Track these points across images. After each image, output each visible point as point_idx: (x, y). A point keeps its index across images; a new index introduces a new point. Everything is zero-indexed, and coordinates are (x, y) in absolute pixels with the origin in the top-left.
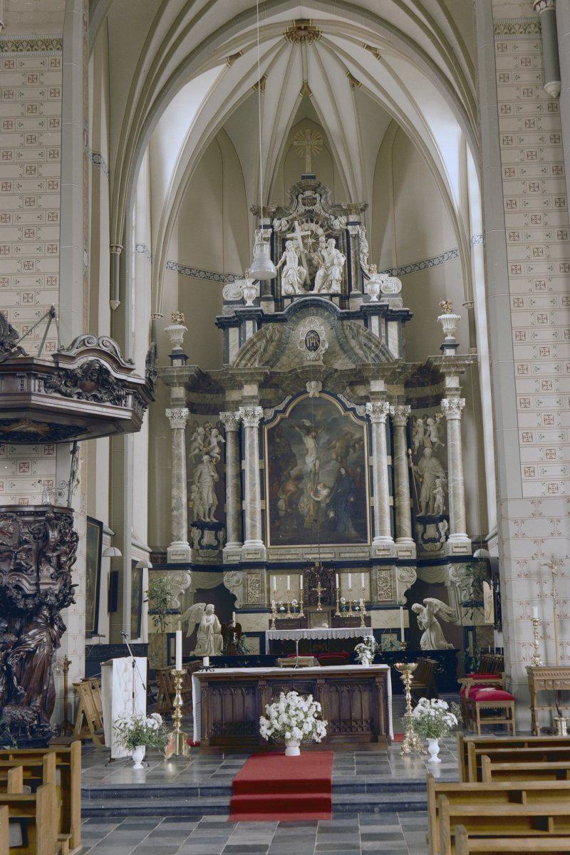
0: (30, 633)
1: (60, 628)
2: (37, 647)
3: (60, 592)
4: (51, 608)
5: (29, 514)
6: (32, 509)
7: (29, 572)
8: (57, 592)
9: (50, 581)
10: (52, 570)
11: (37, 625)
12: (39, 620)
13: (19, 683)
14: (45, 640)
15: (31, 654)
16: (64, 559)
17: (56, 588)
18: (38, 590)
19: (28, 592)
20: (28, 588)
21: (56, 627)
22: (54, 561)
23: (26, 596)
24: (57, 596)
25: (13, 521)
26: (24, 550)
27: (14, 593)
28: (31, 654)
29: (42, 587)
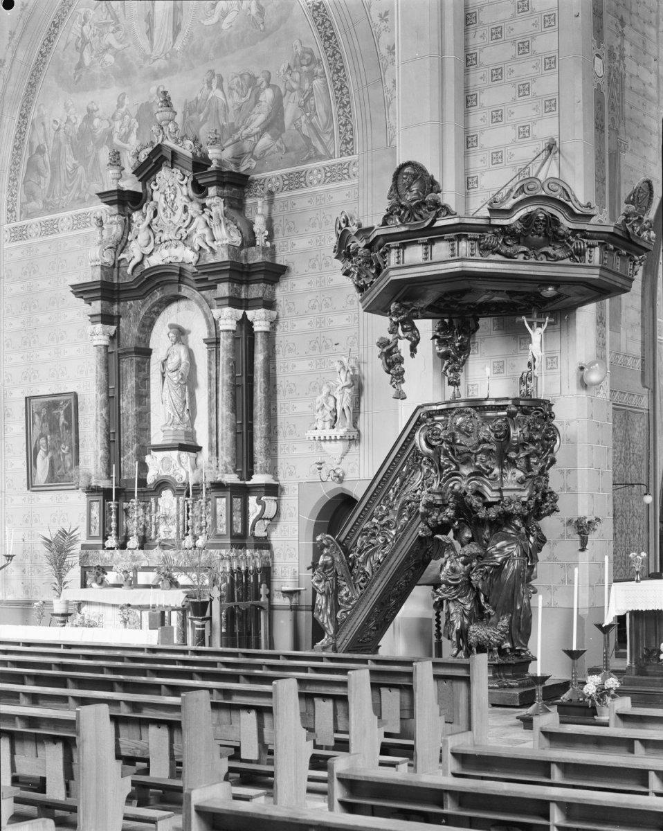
0: (498, 545)
1: (537, 539)
2: (506, 559)
3: (530, 498)
4: (525, 519)
5: (492, 408)
6: (493, 403)
7: (491, 476)
8: (525, 499)
9: (516, 487)
10: (519, 474)
11: (507, 537)
12: (510, 531)
13: (487, 601)
14: (515, 554)
15: (499, 569)
16: (533, 460)
17: (524, 496)
18: (502, 497)
19: (490, 500)
20: (491, 496)
21: (532, 539)
22: (522, 464)
23: (489, 505)
24: (524, 504)
25: (471, 417)
26: (483, 451)
27: (475, 501)
28: (499, 569)
29: (505, 494)
